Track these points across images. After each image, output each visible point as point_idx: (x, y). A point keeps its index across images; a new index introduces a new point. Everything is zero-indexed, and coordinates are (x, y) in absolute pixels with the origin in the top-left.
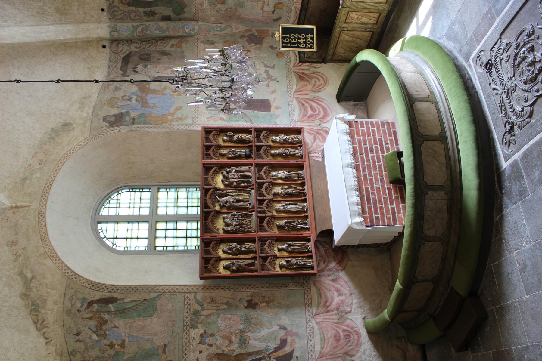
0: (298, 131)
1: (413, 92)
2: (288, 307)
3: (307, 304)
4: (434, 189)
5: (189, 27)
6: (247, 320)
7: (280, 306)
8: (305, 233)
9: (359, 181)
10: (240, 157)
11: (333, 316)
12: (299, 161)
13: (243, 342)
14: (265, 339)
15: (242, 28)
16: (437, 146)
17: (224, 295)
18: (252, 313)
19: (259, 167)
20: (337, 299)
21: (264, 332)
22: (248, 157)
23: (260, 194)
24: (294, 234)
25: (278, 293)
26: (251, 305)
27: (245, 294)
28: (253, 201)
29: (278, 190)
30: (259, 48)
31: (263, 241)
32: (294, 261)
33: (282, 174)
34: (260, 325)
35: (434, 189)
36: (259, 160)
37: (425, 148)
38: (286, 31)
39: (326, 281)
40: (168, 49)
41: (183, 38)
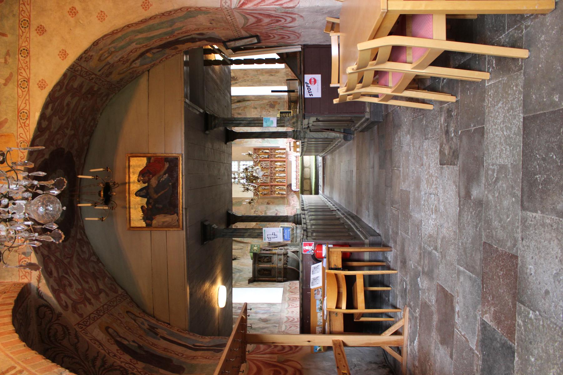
0: (285, 149)
1: (305, 165)
2: (278, 204)
3: (284, 204)
4: (306, 191)
5: (247, 103)
6: (267, 208)
7: (276, 204)
8: (284, 184)
9: (297, 176)
10: (265, 158)
11: (291, 208)
12: (284, 159)
13: (265, 213)
14: (272, 213)
15: (267, 101)
16: (308, 181)
17: (261, 201)
18: (268, 206)
19: (271, 161)
20: (293, 203)
21: (271, 211)
22: (268, 158)
23: (271, 171)
24: (281, 184)
25: (276, 201)
26: (268, 204)
27: (266, 200)
28: (269, 173)
29: (277, 169)
30: (273, 110)
31: (272, 186)
32: (280, 192)
33: (279, 164)
34: (270, 209)
35: (306, 191)
36: (271, 159)
37: (304, 182)
38: (281, 113)
39: (290, 197)
40: (240, 112)
41: (245, 107)
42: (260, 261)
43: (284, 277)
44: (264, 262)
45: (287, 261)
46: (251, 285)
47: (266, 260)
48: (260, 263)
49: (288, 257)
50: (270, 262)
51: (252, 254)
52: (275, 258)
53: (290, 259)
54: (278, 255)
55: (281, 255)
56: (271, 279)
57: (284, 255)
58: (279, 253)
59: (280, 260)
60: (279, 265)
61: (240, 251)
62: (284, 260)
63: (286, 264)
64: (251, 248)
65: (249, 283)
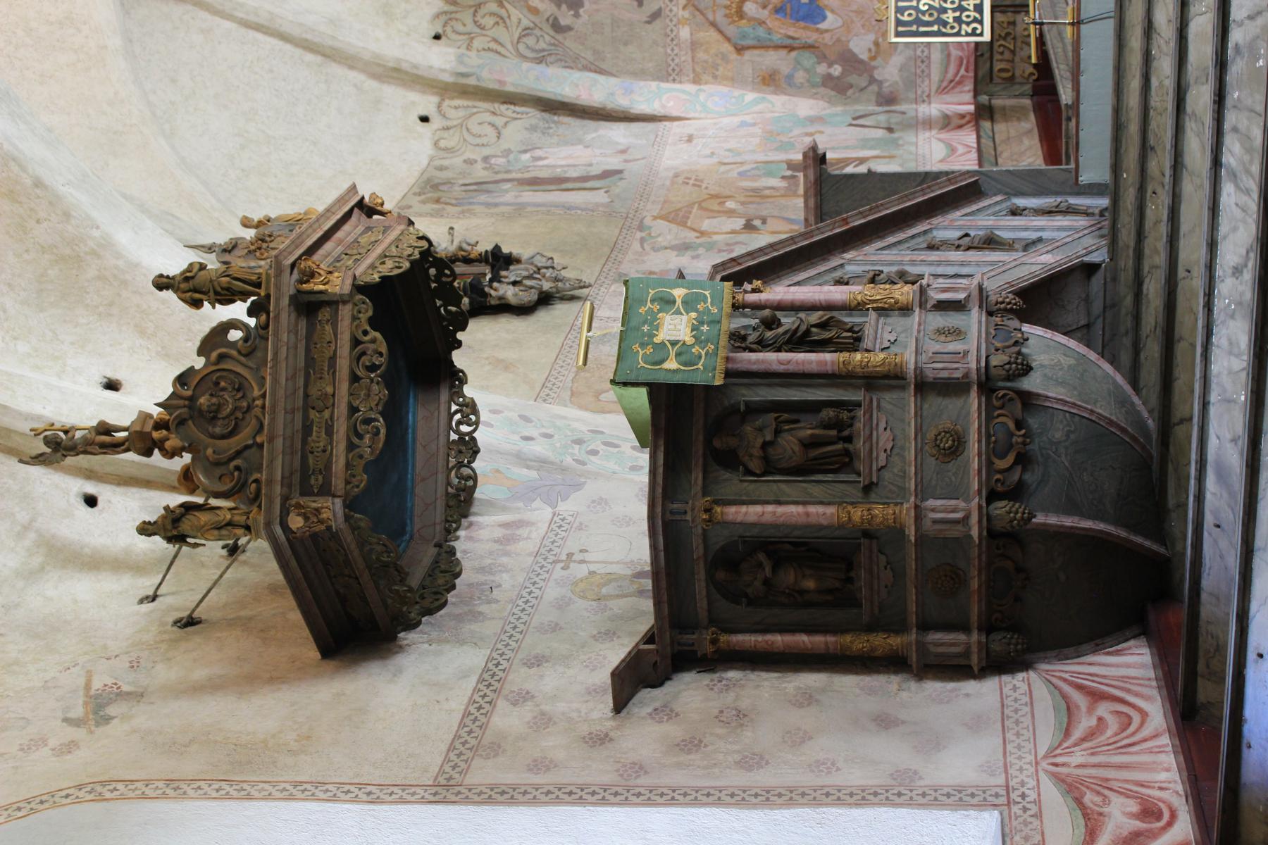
42: (729, 460)
43: (988, 628)
44: (770, 467)
45: (1023, 460)
46: (646, 733)
47: (789, 444)
48: (731, 483)
49: (1027, 399)
50: (845, 462)
51: (640, 397)
52: (893, 429)
53: (1052, 433)
54: (925, 386)
55: (952, 388)
56: (857, 643)
57: (987, 384)
58: (937, 370)
59: (952, 448)
60: (939, 508)
61: (600, 197)
62: (993, 451)
63: (1016, 493)
64: (633, 328)
65: (620, 705)
